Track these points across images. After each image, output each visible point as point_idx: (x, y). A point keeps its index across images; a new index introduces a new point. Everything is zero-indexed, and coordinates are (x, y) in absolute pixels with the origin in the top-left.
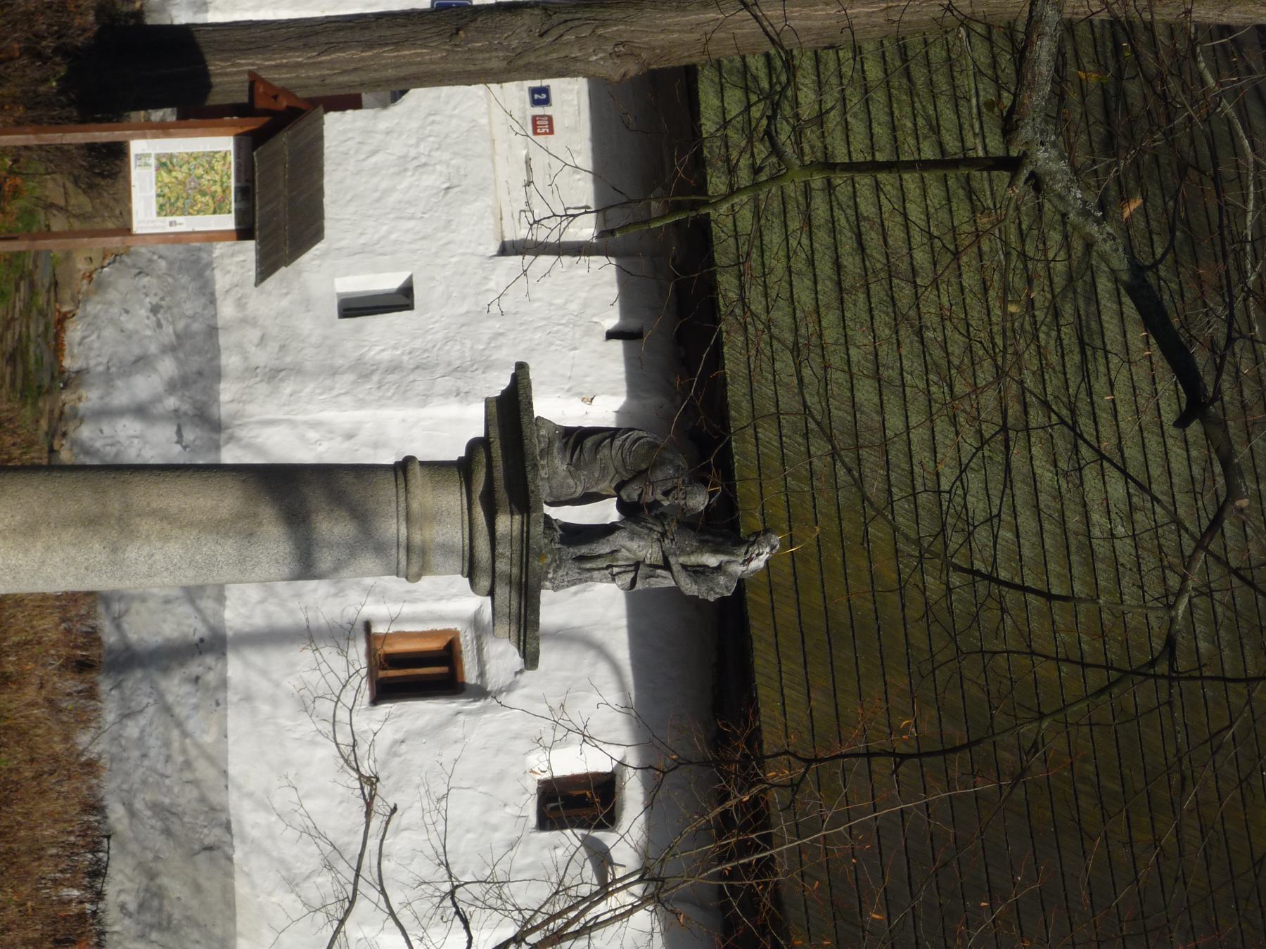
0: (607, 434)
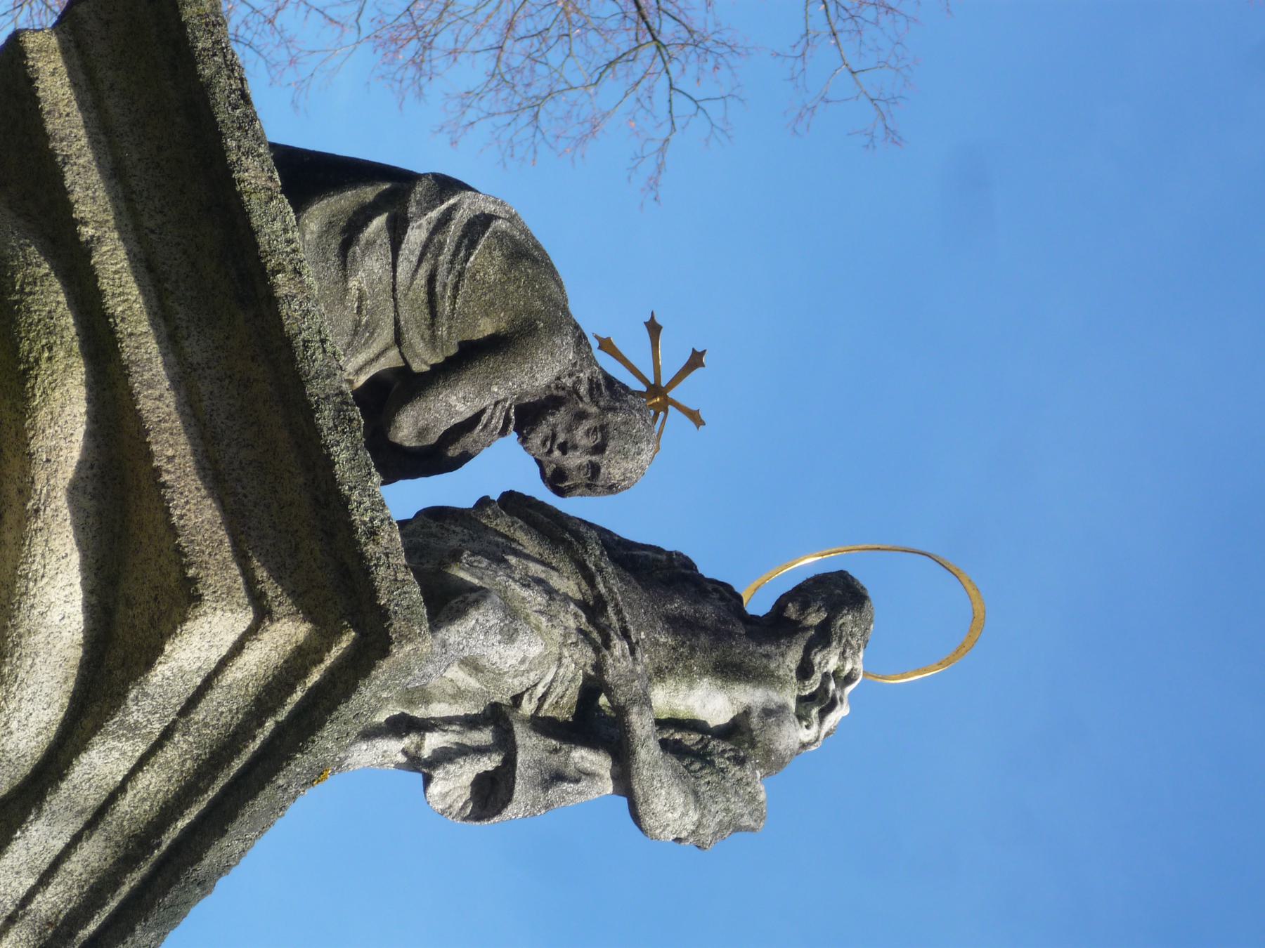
0: (369, 193)
